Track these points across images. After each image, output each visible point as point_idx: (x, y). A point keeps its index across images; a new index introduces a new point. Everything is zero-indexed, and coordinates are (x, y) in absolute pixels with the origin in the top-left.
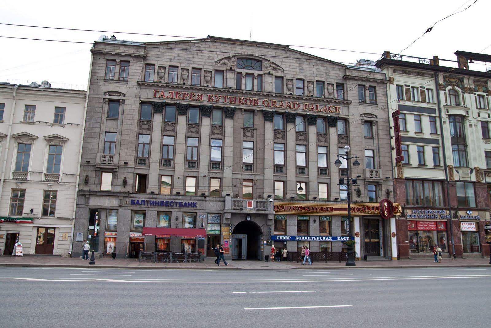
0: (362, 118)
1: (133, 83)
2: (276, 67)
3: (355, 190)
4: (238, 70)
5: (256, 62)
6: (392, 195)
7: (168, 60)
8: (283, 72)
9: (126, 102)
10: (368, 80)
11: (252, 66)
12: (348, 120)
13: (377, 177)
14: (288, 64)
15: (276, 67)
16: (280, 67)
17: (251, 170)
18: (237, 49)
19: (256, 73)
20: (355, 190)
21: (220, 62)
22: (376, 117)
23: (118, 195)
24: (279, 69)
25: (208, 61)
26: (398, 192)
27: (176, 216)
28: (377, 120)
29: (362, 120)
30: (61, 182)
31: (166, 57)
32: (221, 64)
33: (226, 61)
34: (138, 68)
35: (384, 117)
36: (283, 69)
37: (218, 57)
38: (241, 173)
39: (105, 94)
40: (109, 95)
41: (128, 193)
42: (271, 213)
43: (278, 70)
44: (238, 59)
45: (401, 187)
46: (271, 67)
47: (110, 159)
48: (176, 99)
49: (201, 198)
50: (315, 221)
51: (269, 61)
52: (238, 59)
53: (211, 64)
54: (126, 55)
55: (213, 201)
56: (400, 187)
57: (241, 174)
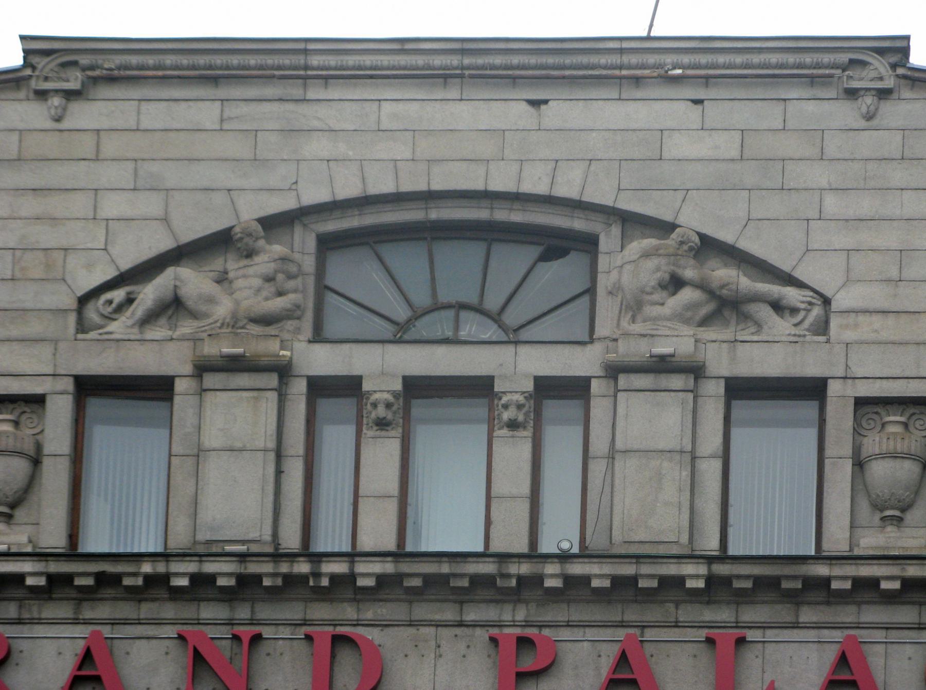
2: (745, 283)
5: (534, 252)
8: (822, 327)
11: (493, 302)
15: (745, 283)
16: (790, 280)
21: (130, 301)
24: (778, 307)
32: (150, 319)
36: (827, 301)
37: (115, 251)
43: (764, 312)
46: (687, 295)
51: (666, 228)
53: (35, 328)
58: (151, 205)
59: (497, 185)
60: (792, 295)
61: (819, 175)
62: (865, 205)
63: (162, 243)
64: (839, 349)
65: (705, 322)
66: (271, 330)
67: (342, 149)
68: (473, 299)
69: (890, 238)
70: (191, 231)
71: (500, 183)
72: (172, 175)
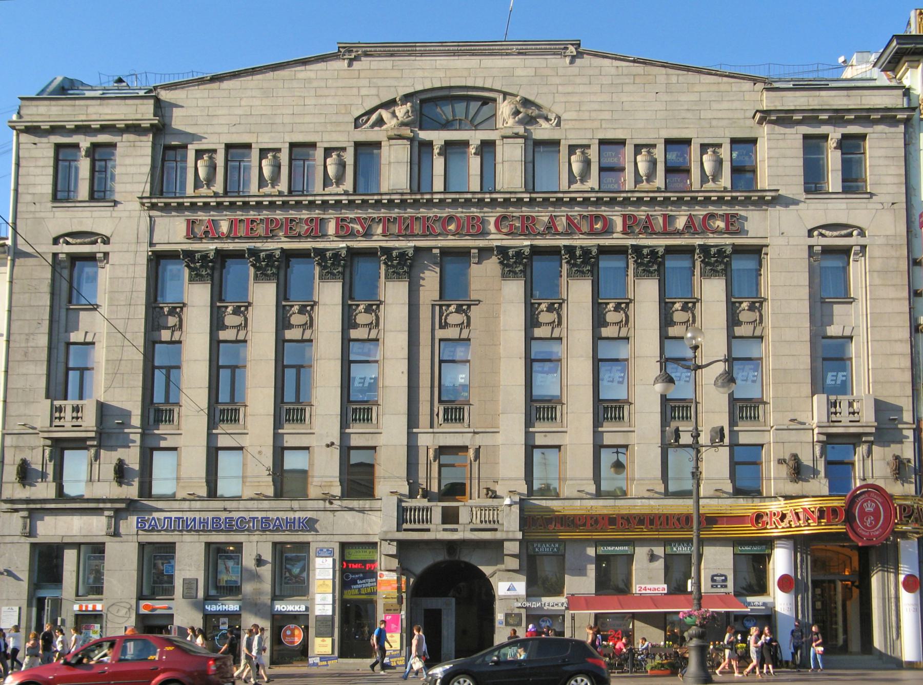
0: (812, 241)
3: (781, 461)
7: (225, 129)
8: (558, 124)
13: (856, 417)
14: (576, 99)
17: (461, 420)
18: (419, 73)
19: (475, 137)
20: (781, 461)
23: (101, 505)
25: (334, 119)
27: (255, 553)
28: (862, 241)
29: (811, 247)
31: (215, 121)
33: (385, 114)
34: (140, 161)
35: (891, 231)
37: (365, 104)
38: (431, 430)
39: (56, 241)
40: (68, 243)
44: (422, 101)
47: (75, 415)
48: (248, 238)
49: (321, 504)
50: (653, 558)
51: (516, 96)
52: (422, 101)
55: (352, 509)
57: (433, 433)
58: (374, 91)
59: (469, 84)
61: (557, 80)
62: (569, 89)
63: (377, 102)
64: (564, 131)
67: (426, 74)
69: (576, 99)
70: (386, 98)
71: (470, 83)
72: (380, 83)
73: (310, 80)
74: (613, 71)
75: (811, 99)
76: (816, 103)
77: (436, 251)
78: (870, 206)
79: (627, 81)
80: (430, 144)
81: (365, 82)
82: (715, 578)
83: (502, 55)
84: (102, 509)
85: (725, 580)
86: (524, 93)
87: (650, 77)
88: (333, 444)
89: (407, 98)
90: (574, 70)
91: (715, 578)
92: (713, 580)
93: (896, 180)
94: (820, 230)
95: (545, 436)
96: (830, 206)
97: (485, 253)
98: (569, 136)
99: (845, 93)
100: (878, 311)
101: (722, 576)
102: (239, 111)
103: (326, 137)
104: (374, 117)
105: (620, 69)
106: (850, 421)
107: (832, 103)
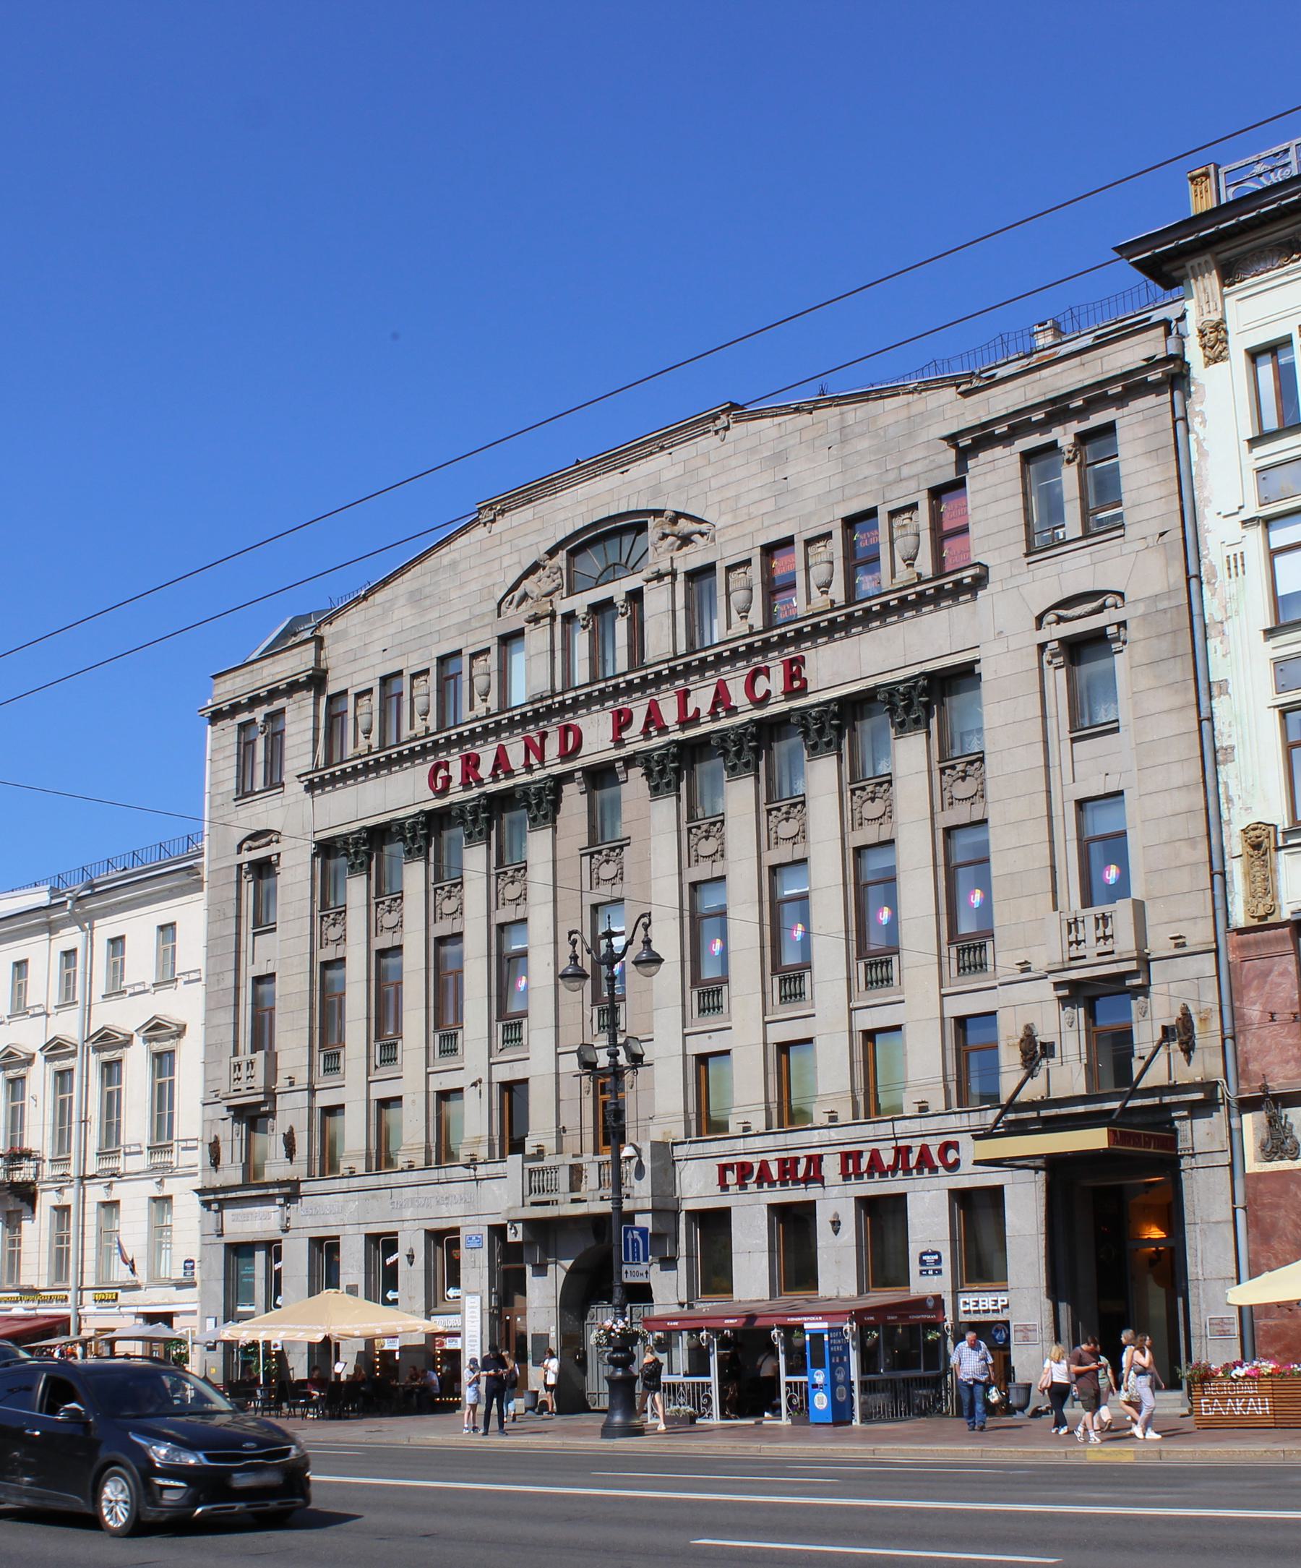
0: (1043, 636)
1: (295, 788)
4: (563, 606)
6: (1208, 1036)
8: (713, 540)
9: (284, 861)
10: (1058, 410)
12: (978, 669)
16: (701, 521)
18: (561, 516)
19: (617, 590)
22: (1121, 595)
23: (271, 1191)
24: (702, 534)
26: (1254, 1012)
30: (177, 1168)
33: (527, 585)
35: (1158, 587)
41: (295, 1184)
42: (639, 1207)
44: (572, 554)
45: (1273, 977)
46: (671, 539)
53: (487, 620)
54: (274, 694)
56: (1266, 974)
58: (515, 558)
60: (704, 527)
61: (708, 472)
63: (518, 573)
65: (679, 548)
66: (548, 599)
68: (617, 561)
69: (730, 493)
70: (527, 564)
73: (453, 564)
74: (774, 433)
75: (1028, 388)
76: (1035, 393)
77: (579, 774)
78: (1128, 548)
79: (791, 442)
80: (569, 617)
81: (506, 548)
82: (924, 1258)
83: (646, 456)
84: (273, 1196)
85: (938, 1262)
86: (671, 506)
87: (821, 425)
88: (480, 1081)
89: (552, 553)
90: (728, 449)
91: (924, 1258)
92: (922, 1262)
93: (1162, 492)
94: (1056, 611)
95: (710, 1037)
96: (1066, 566)
97: (629, 761)
98: (724, 554)
99: (1076, 361)
100: (1150, 738)
101: (934, 1253)
102: (392, 630)
103: (471, 640)
104: (517, 594)
105: (783, 426)
106: (1099, 955)
107: (1059, 384)
